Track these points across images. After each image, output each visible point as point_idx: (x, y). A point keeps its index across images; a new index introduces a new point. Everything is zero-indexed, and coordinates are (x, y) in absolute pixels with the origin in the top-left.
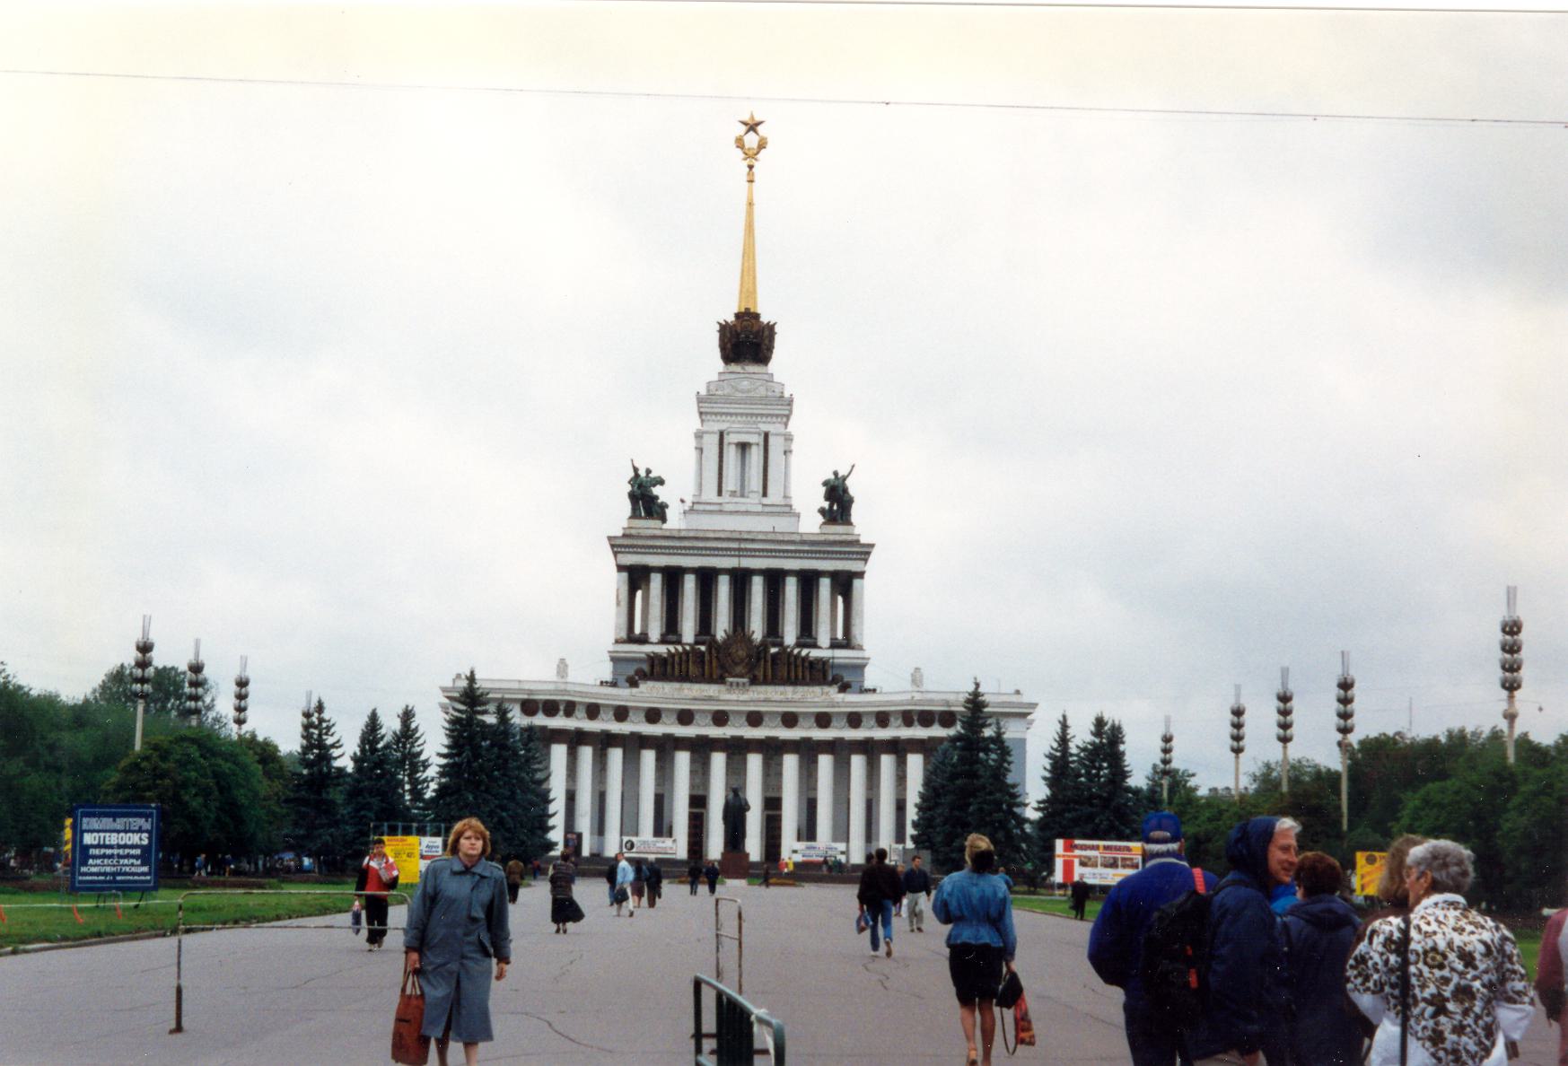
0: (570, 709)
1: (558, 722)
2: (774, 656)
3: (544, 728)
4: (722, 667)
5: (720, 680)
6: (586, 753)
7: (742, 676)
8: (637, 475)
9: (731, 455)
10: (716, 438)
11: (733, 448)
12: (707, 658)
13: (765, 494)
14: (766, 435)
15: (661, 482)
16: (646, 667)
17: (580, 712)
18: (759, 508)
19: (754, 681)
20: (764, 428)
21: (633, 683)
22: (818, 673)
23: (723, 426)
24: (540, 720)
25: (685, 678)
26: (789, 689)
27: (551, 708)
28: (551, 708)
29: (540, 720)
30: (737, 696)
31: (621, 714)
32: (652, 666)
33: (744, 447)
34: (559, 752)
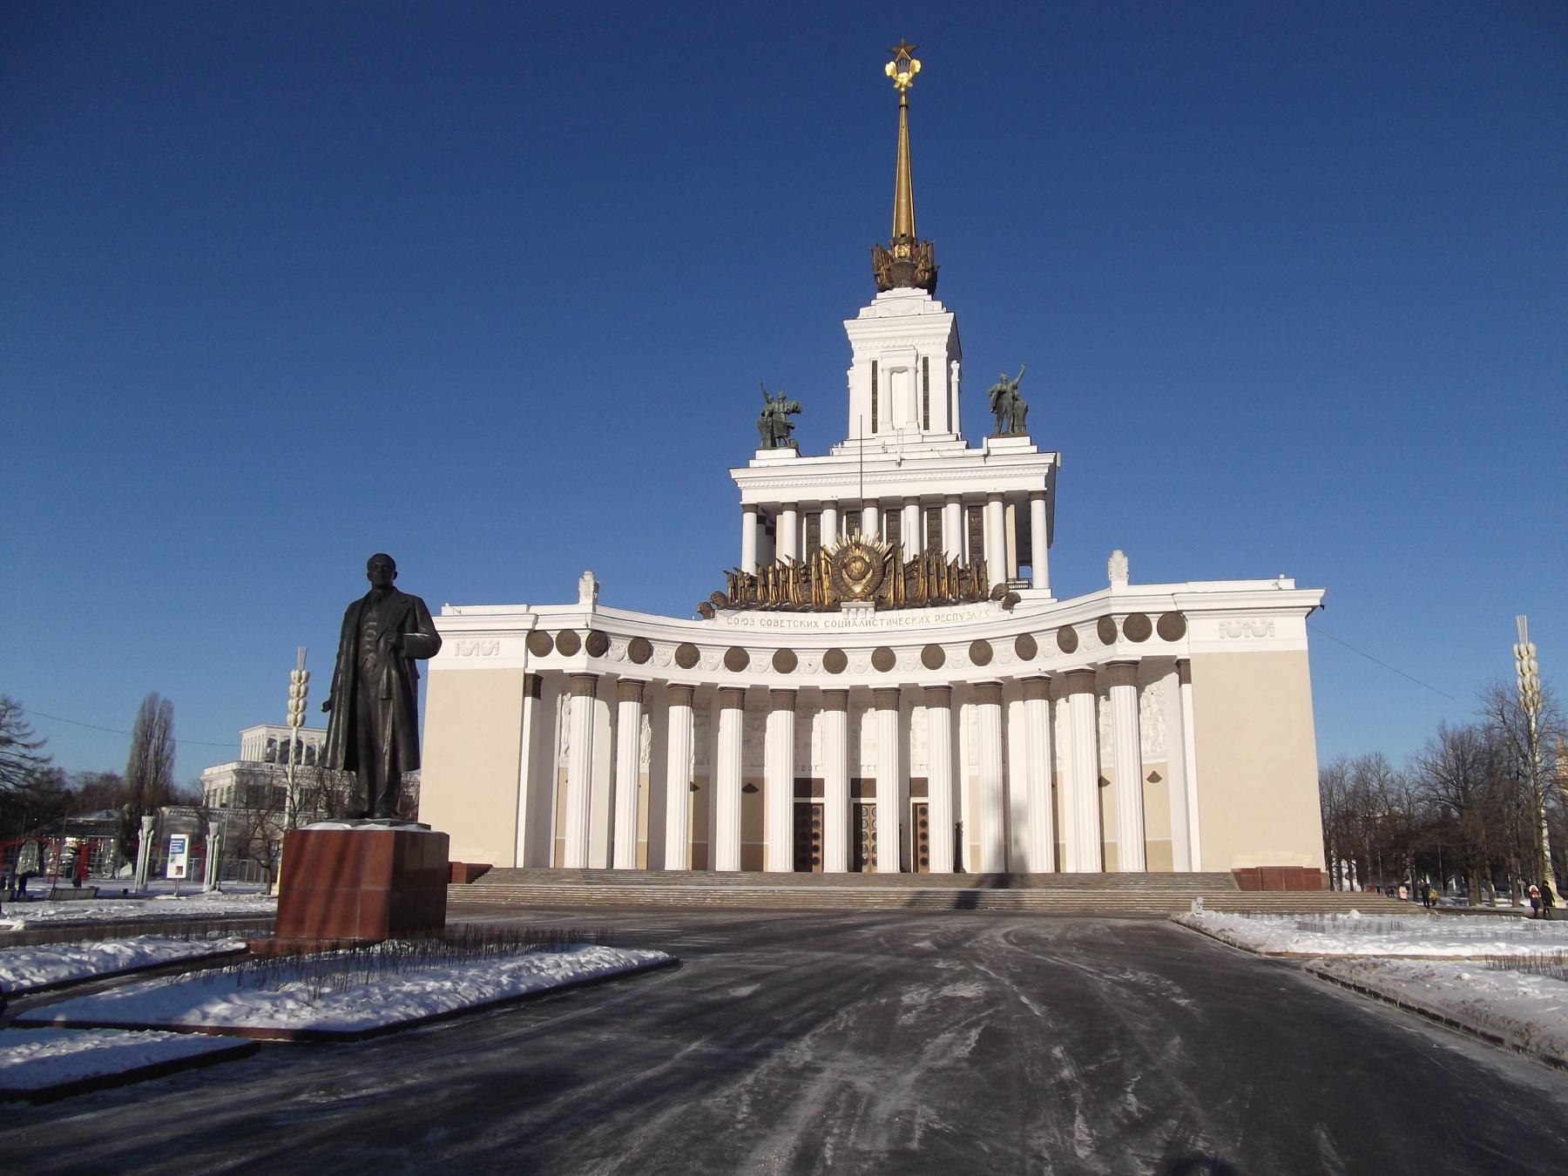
0: (599, 643)
1: (579, 662)
3: (557, 675)
4: (837, 583)
5: (835, 607)
7: (864, 599)
11: (887, 373)
13: (926, 427)
14: (926, 360)
15: (795, 411)
17: (619, 648)
19: (881, 605)
20: (923, 352)
21: (707, 612)
23: (875, 355)
24: (555, 661)
25: (783, 606)
26: (931, 612)
27: (568, 642)
28: (568, 642)
29: (555, 661)
30: (858, 626)
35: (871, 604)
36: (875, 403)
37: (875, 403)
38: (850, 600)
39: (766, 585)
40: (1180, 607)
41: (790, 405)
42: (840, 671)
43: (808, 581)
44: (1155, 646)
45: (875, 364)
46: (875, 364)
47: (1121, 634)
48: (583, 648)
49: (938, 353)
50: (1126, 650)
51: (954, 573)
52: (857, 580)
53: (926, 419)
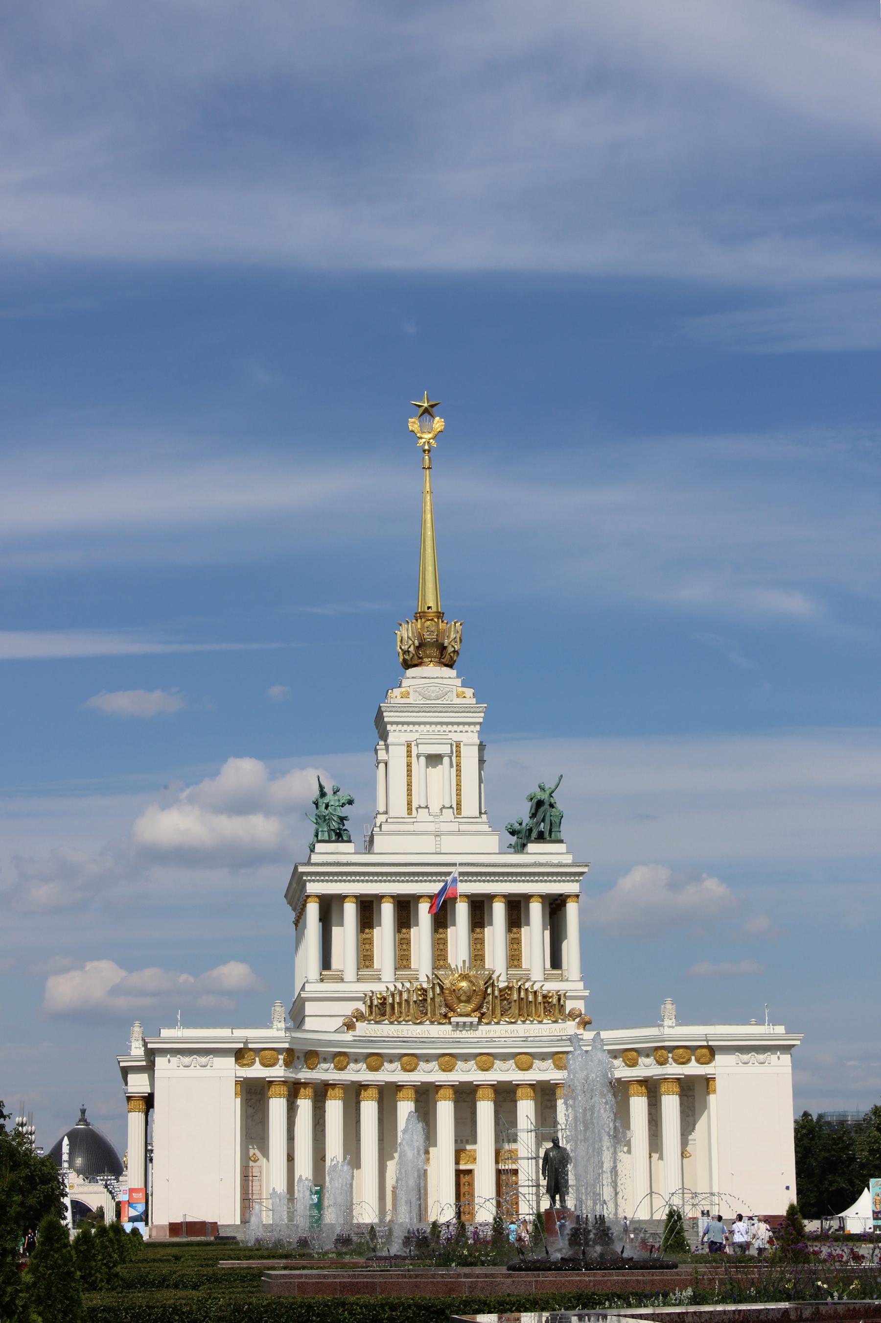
1: (278, 1072)
2: (501, 990)
6: (305, 1106)
7: (468, 1015)
8: (323, 794)
9: (419, 766)
10: (404, 749)
11: (423, 760)
12: (430, 994)
14: (458, 746)
15: (350, 802)
16: (363, 1008)
18: (454, 827)
20: (456, 737)
22: (551, 1007)
23: (412, 737)
24: (257, 1071)
31: (341, 1059)
32: (371, 1007)
33: (434, 760)
34: (277, 1106)
35: (476, 1019)
36: (409, 785)
37: (409, 785)
38: (461, 1015)
39: (392, 1005)
40: (711, 1043)
41: (343, 796)
42: (450, 1071)
43: (425, 1000)
44: (693, 1069)
45: (409, 746)
46: (409, 746)
47: (670, 1060)
48: (281, 1062)
49: (470, 738)
50: (673, 1069)
51: (540, 999)
52: (460, 1001)
53: (459, 804)
